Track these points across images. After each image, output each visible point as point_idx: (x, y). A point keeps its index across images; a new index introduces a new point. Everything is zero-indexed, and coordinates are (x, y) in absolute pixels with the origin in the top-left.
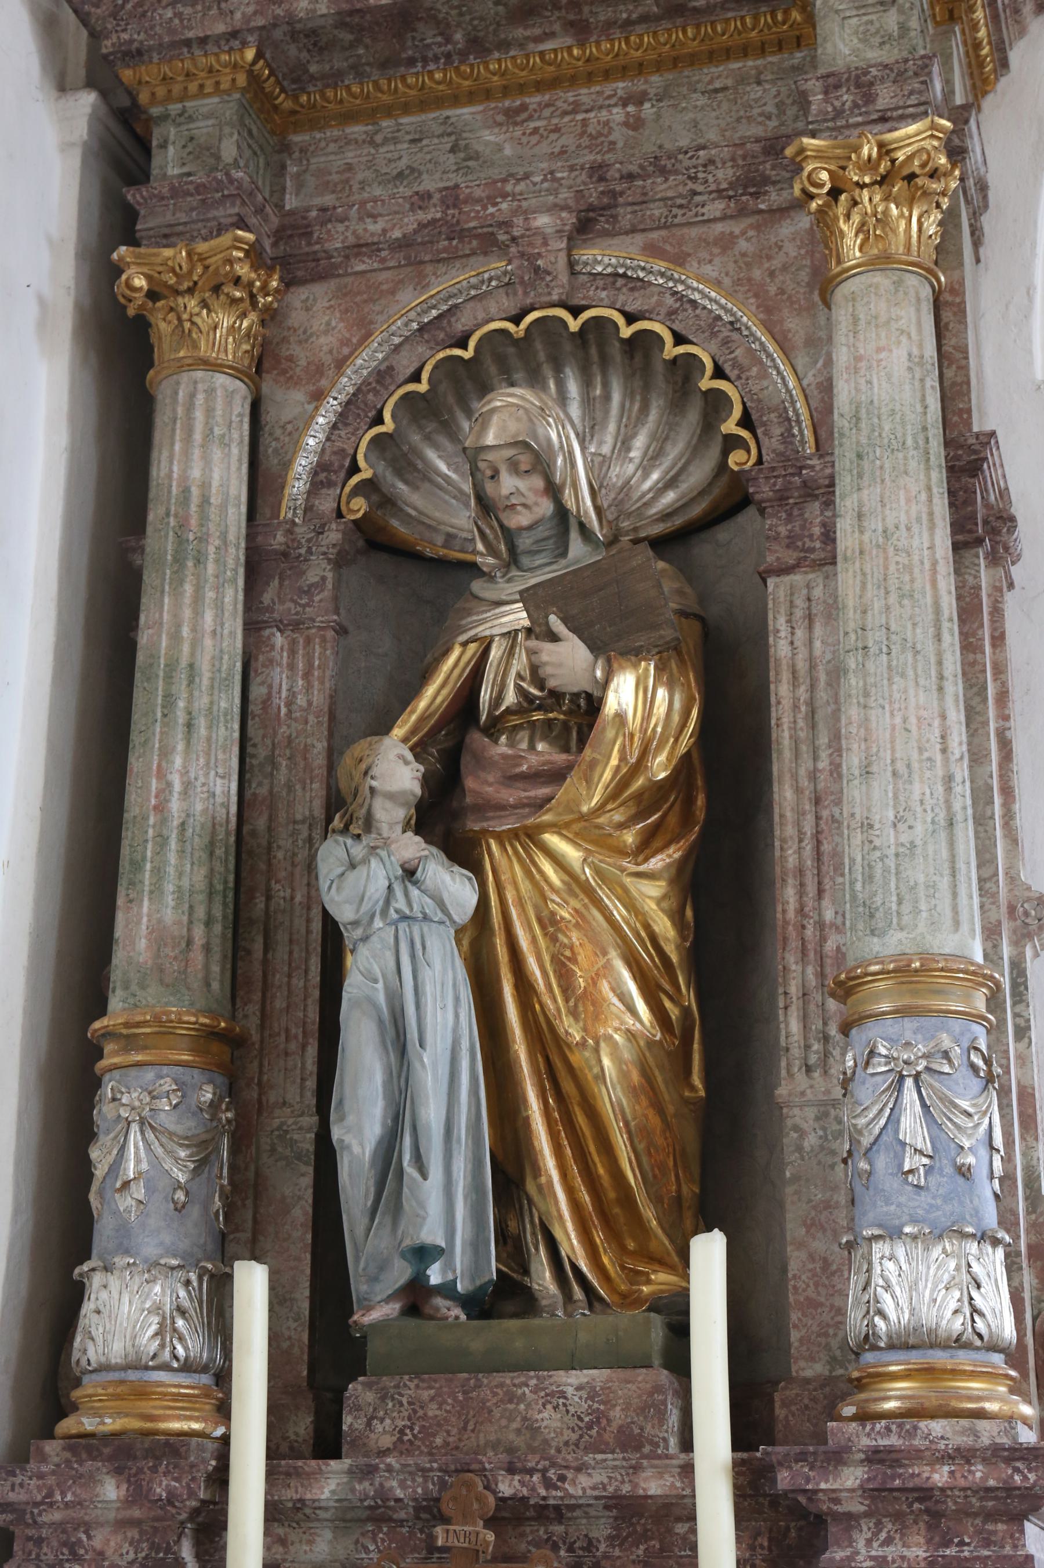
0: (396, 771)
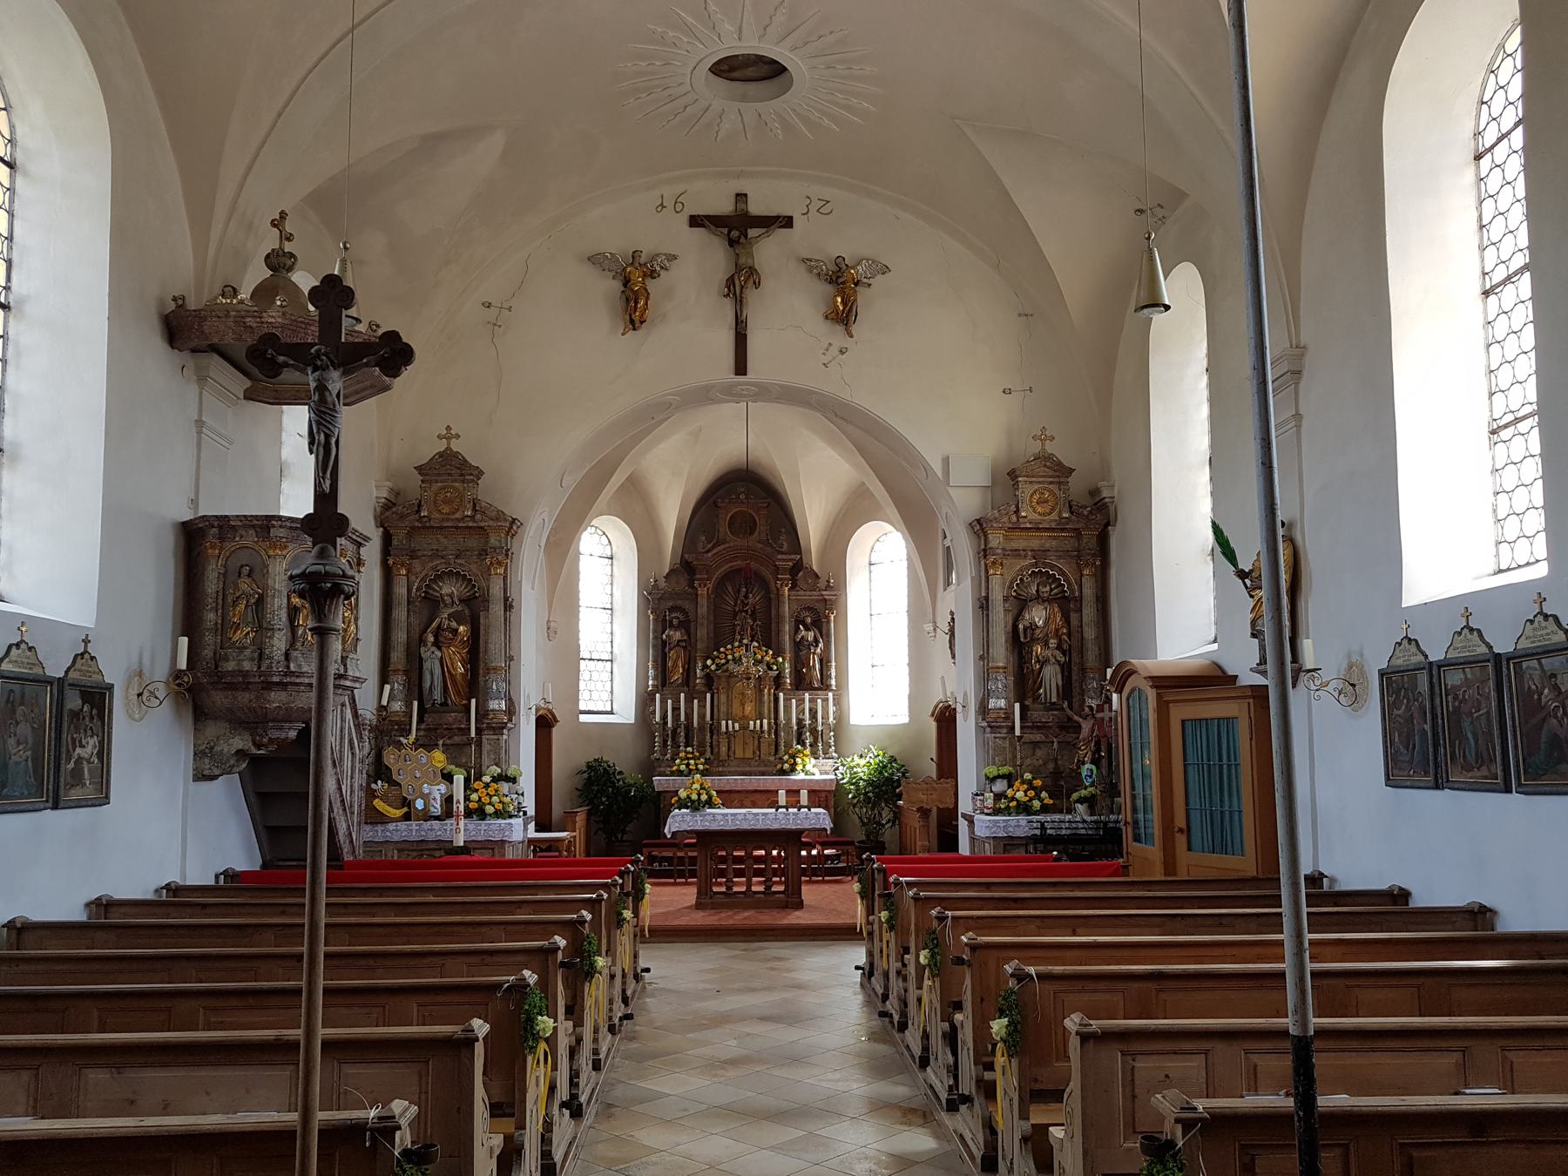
0: (431, 639)
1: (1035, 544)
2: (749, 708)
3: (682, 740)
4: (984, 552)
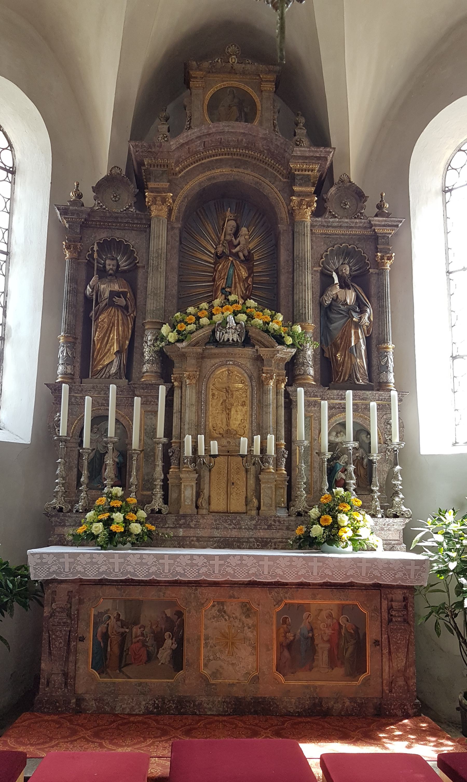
2: (239, 416)
3: (109, 472)
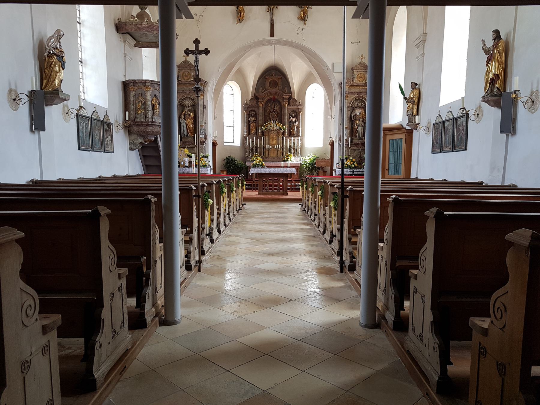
0: (183, 117)
1: (358, 90)
2: (275, 142)
3: (255, 151)
4: (342, 94)
